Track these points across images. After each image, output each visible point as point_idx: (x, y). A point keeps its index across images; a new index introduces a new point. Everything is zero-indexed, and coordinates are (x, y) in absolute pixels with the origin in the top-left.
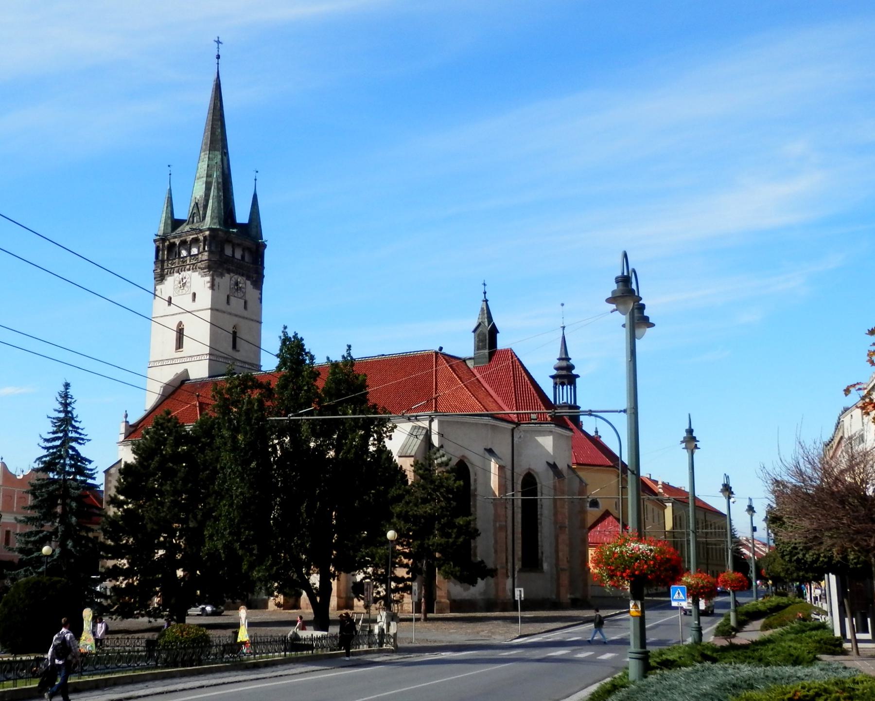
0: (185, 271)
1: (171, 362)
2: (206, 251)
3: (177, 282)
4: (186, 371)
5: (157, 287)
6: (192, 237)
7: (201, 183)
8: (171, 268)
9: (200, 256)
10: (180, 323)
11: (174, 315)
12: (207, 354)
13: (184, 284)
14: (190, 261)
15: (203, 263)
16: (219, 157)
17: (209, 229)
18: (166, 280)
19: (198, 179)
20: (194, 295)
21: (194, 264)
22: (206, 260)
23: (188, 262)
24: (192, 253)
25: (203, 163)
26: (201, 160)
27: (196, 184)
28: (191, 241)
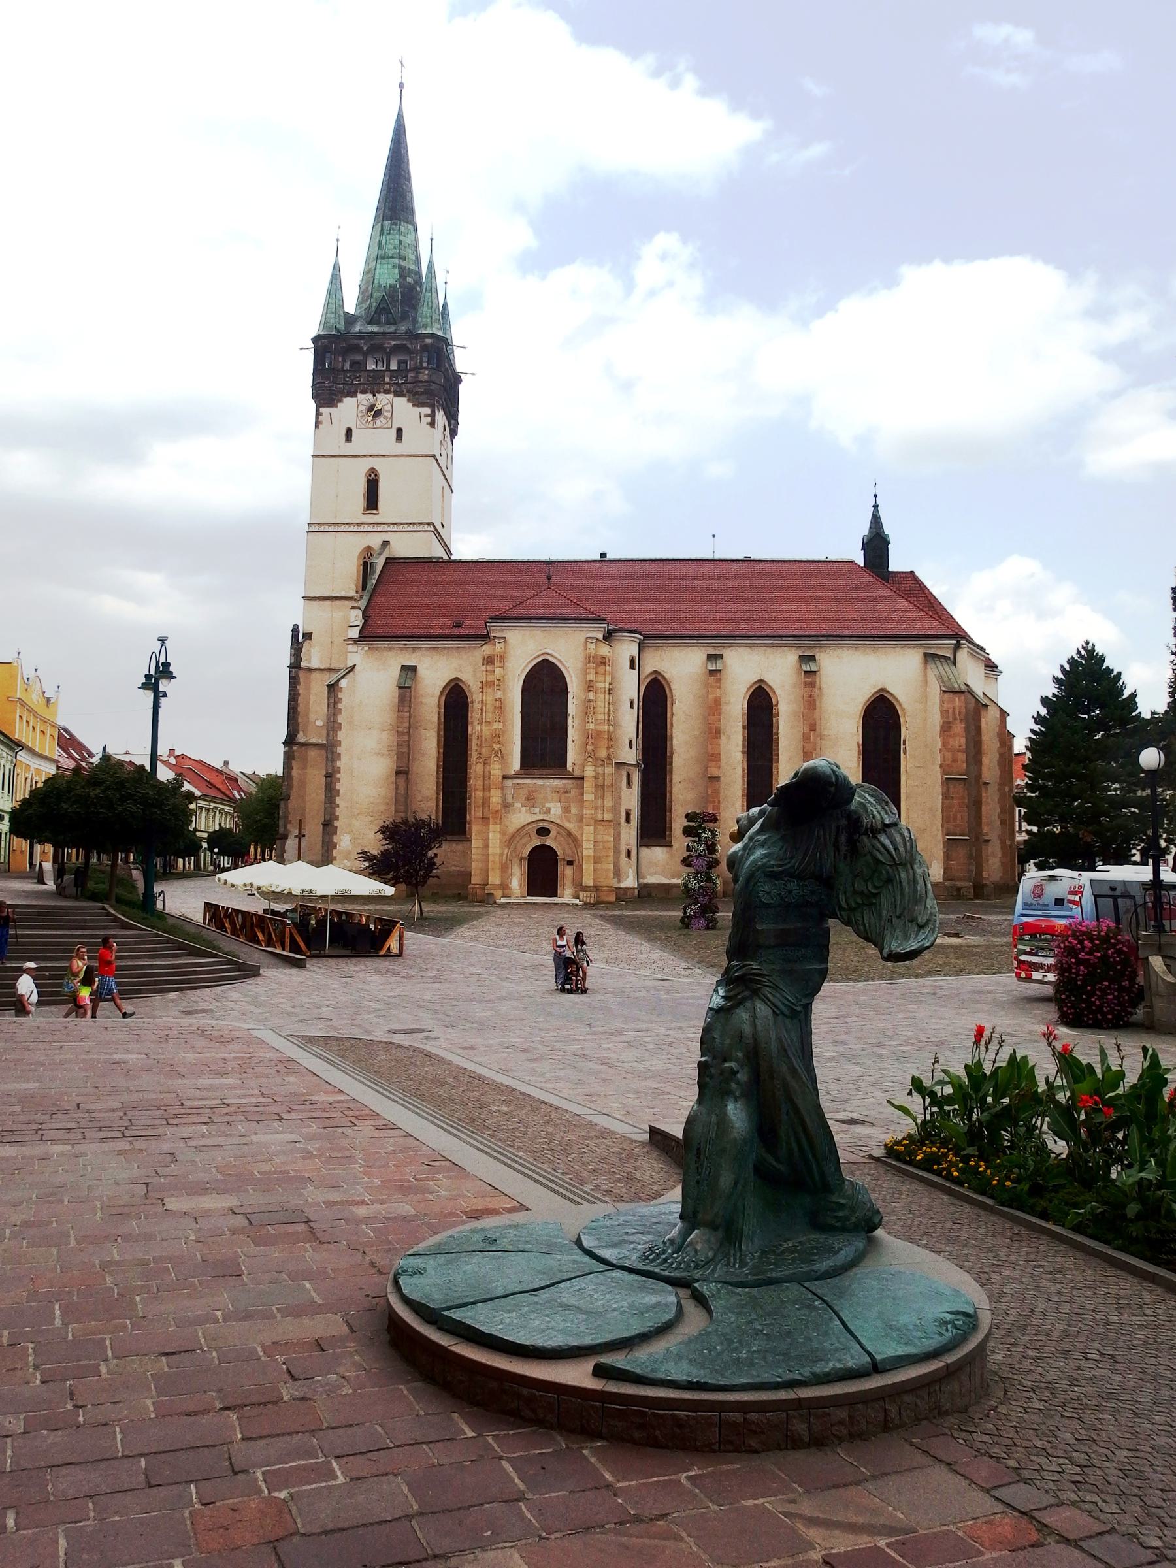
0: (379, 392)
1: (356, 528)
2: (425, 368)
3: (363, 408)
4: (386, 544)
5: (322, 410)
6: (393, 343)
7: (390, 266)
8: (352, 384)
9: (411, 374)
10: (373, 470)
11: (359, 456)
12: (428, 524)
13: (378, 414)
14: (391, 380)
15: (421, 384)
16: (413, 233)
17: (432, 335)
18: (340, 401)
19: (382, 258)
20: (399, 431)
21: (398, 383)
22: (425, 382)
23: (387, 379)
24: (391, 368)
25: (391, 237)
26: (385, 232)
27: (378, 266)
28: (391, 348)
